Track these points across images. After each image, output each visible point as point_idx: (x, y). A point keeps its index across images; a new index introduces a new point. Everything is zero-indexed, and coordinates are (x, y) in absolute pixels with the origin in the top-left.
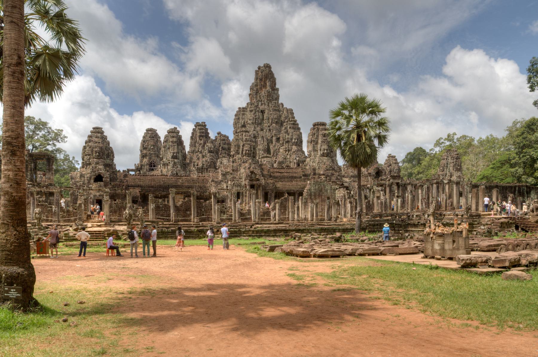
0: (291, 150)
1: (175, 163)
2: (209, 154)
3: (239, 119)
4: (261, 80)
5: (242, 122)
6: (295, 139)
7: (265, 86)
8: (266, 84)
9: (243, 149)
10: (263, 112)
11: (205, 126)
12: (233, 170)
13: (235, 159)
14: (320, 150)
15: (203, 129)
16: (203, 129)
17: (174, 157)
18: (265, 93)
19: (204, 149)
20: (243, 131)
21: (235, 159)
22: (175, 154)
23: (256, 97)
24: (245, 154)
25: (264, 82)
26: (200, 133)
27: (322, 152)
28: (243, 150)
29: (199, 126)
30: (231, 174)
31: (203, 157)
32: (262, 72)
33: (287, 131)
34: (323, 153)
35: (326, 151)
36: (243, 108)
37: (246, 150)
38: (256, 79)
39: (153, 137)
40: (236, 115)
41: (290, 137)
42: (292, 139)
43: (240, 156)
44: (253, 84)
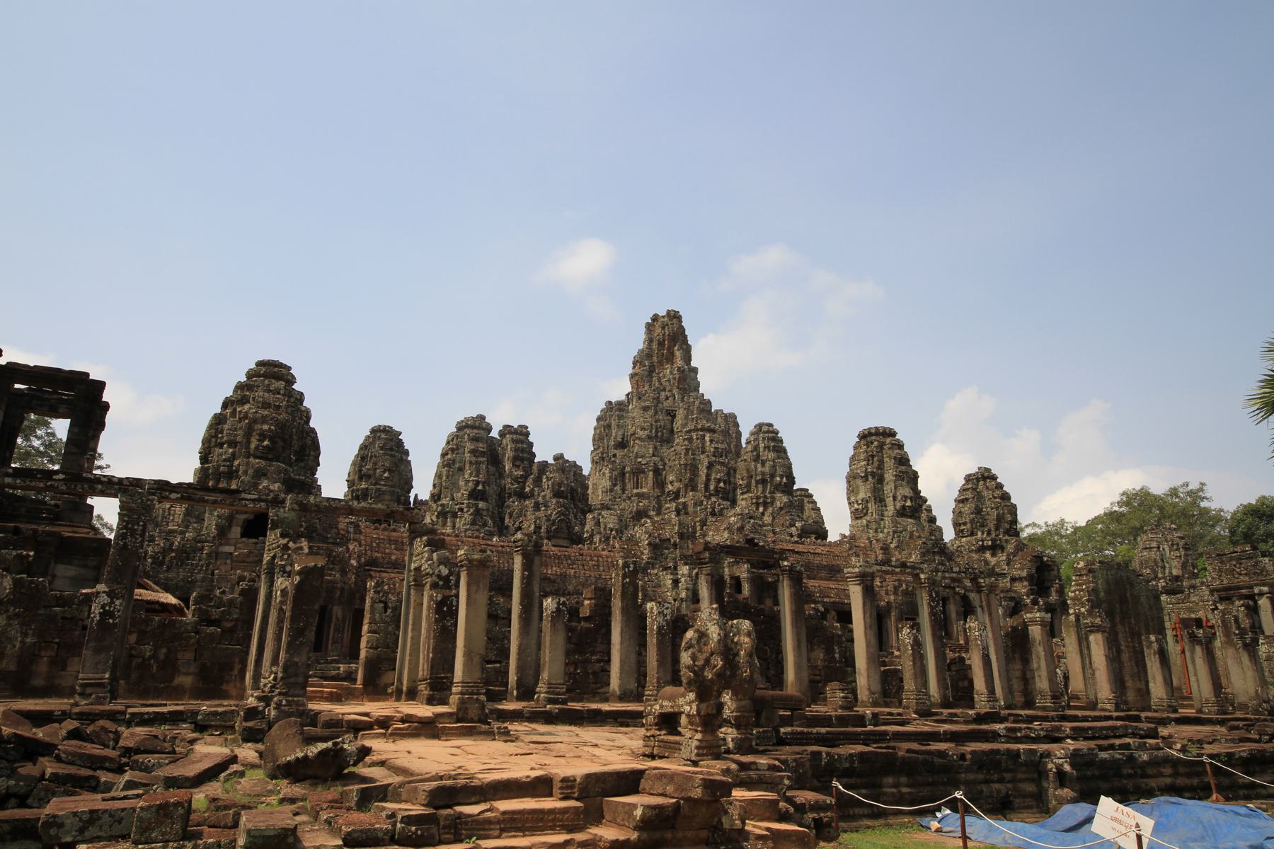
0: (772, 503)
1: (478, 512)
2: (554, 501)
3: (609, 426)
4: (661, 344)
5: (616, 434)
6: (782, 477)
7: (670, 358)
8: (673, 354)
9: (708, 475)
10: (671, 414)
11: (528, 434)
12: (681, 536)
13: (685, 504)
14: (895, 498)
15: (522, 442)
16: (522, 442)
17: (474, 495)
18: (671, 373)
19: (540, 486)
20: (703, 429)
21: (685, 504)
22: (480, 487)
23: (650, 381)
24: (717, 490)
25: (669, 349)
26: (516, 450)
27: (899, 505)
28: (708, 480)
29: (510, 433)
30: (675, 545)
31: (537, 507)
32: (663, 328)
33: (758, 456)
34: (904, 507)
35: (909, 503)
36: (620, 403)
37: (719, 481)
38: (650, 341)
39: (391, 449)
40: (599, 419)
41: (767, 469)
42: (773, 476)
43: (700, 495)
44: (641, 351)
